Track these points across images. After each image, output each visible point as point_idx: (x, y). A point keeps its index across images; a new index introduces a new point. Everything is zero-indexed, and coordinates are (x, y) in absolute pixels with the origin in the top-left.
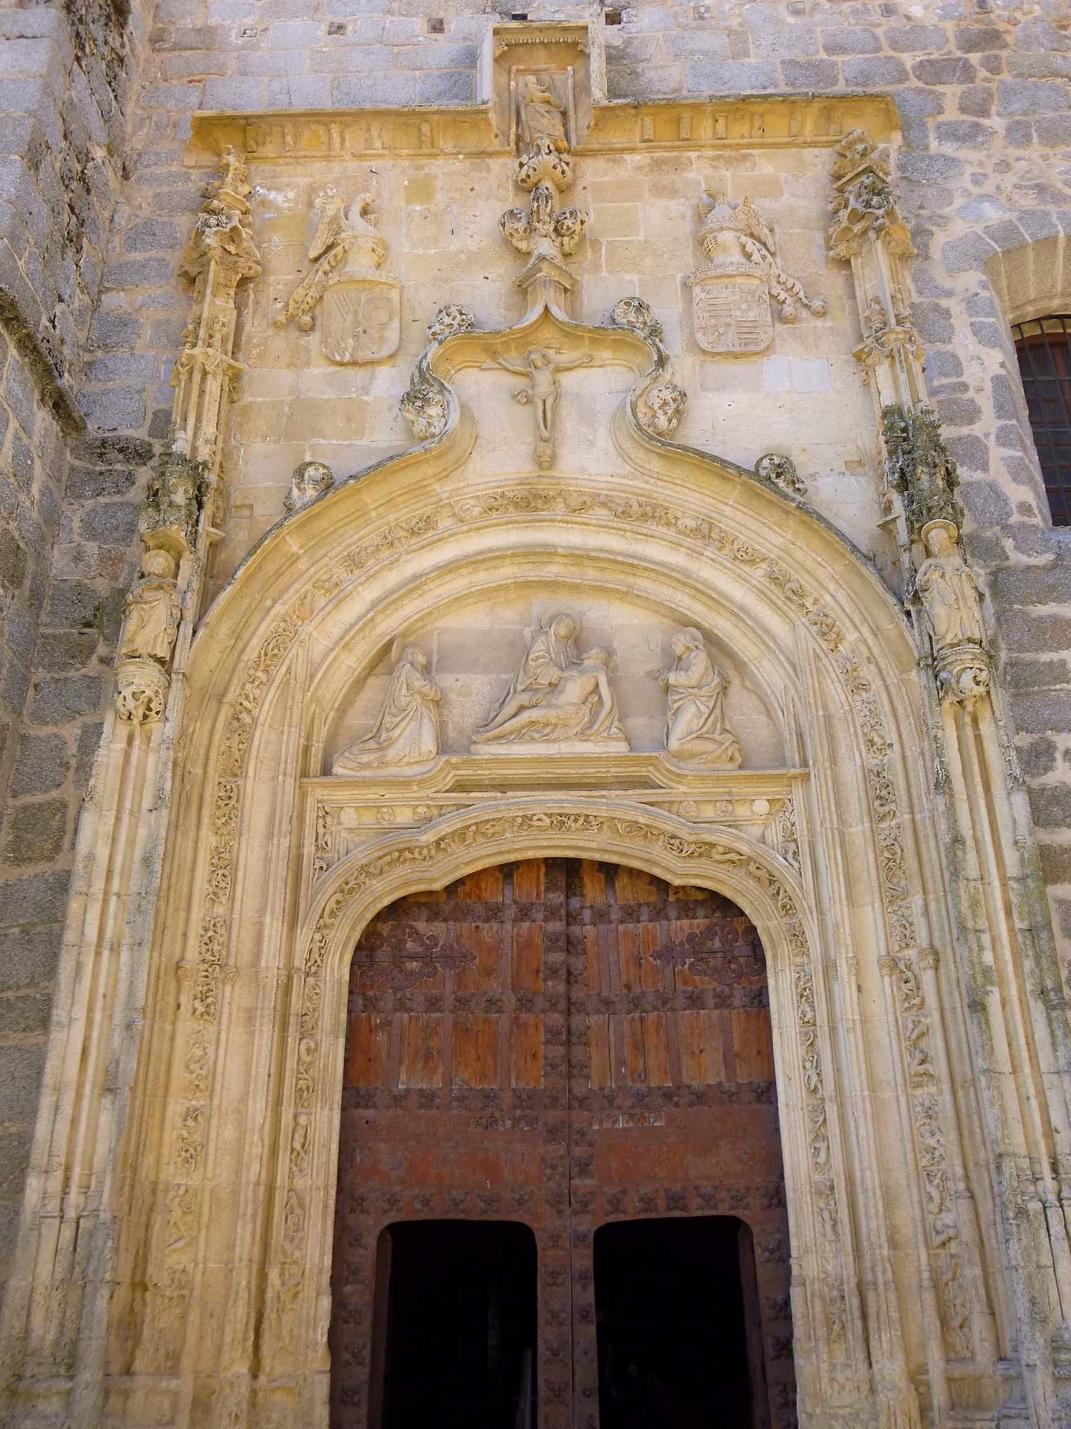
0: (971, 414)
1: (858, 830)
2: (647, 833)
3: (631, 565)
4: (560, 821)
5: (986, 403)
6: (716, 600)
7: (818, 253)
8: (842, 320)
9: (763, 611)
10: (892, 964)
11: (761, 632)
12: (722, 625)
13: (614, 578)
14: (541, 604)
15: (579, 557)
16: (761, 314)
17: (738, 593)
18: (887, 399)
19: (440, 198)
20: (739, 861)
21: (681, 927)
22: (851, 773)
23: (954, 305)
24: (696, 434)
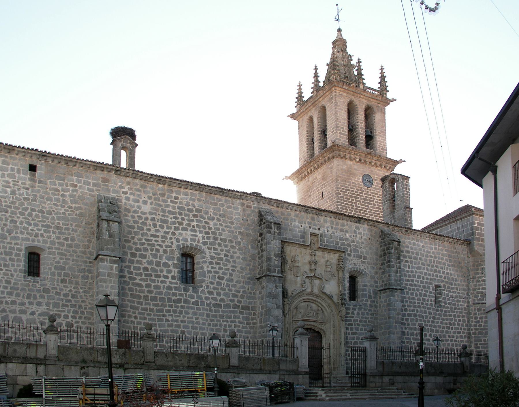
0: (345, 290)
1: (332, 328)
2: (316, 327)
3: (316, 301)
4: (310, 325)
5: (347, 290)
6: (323, 306)
7: (336, 268)
8: (337, 278)
9: (326, 307)
10: (333, 340)
11: (326, 310)
12: (323, 308)
13: (314, 302)
14: (307, 303)
15: (312, 300)
16: (330, 276)
17: (325, 305)
18: (340, 290)
19: (303, 254)
20: (322, 330)
21: (316, 334)
22: (332, 323)
23: (346, 277)
24: (324, 291)
